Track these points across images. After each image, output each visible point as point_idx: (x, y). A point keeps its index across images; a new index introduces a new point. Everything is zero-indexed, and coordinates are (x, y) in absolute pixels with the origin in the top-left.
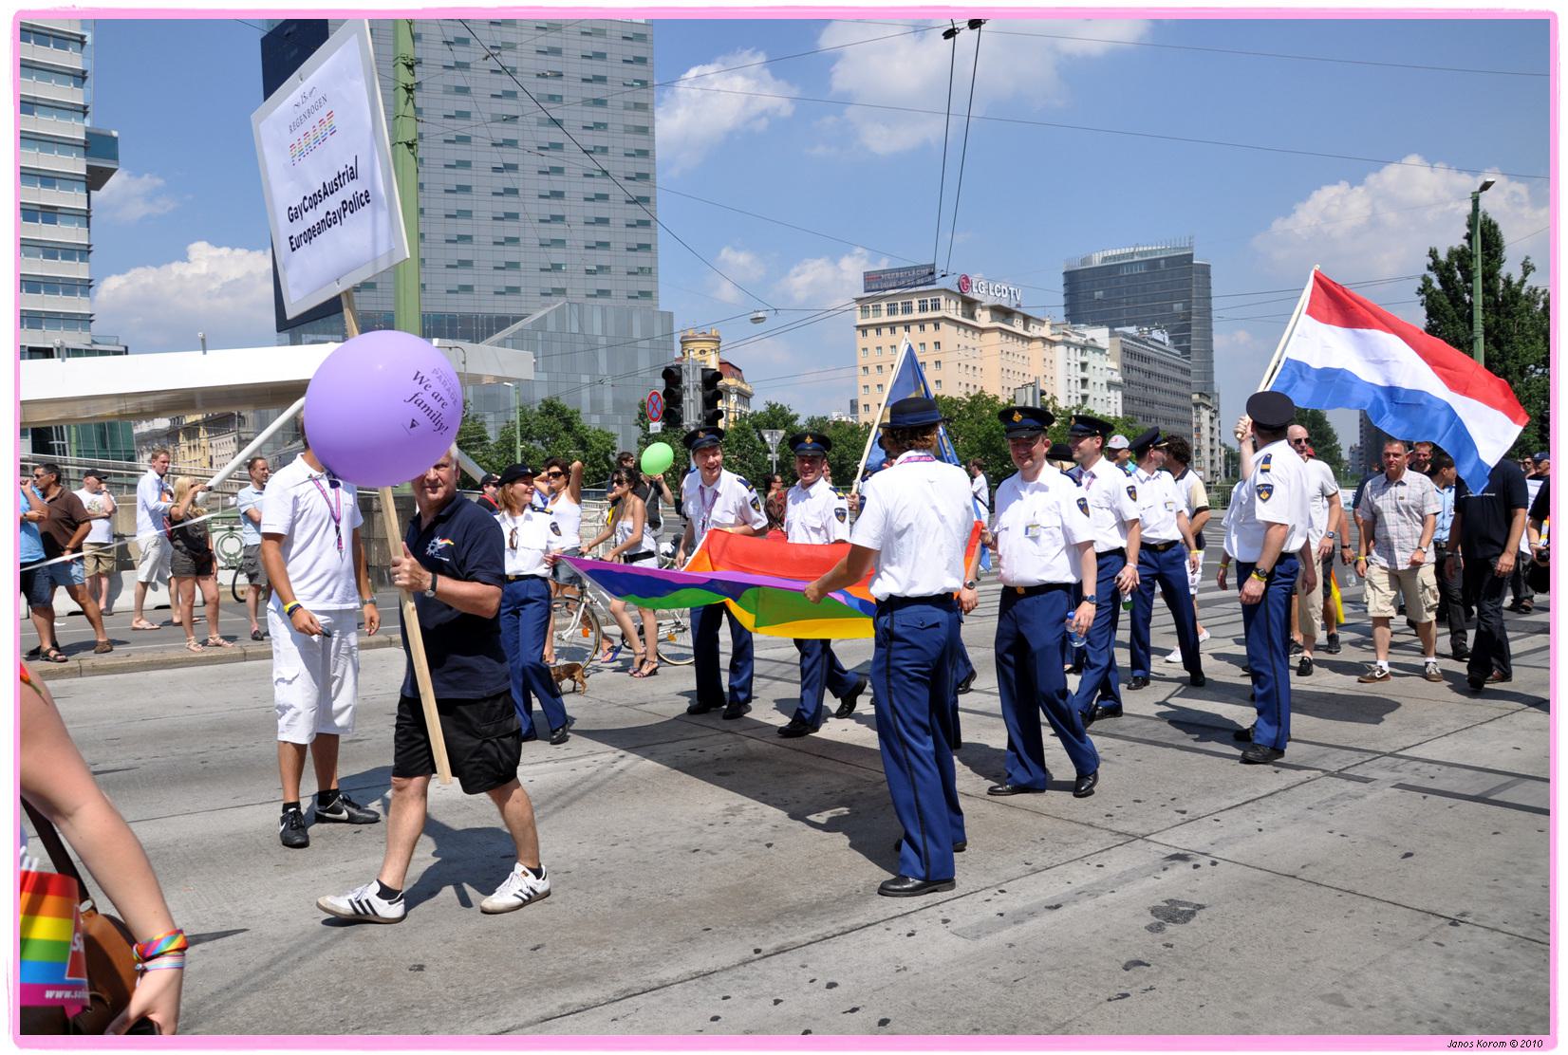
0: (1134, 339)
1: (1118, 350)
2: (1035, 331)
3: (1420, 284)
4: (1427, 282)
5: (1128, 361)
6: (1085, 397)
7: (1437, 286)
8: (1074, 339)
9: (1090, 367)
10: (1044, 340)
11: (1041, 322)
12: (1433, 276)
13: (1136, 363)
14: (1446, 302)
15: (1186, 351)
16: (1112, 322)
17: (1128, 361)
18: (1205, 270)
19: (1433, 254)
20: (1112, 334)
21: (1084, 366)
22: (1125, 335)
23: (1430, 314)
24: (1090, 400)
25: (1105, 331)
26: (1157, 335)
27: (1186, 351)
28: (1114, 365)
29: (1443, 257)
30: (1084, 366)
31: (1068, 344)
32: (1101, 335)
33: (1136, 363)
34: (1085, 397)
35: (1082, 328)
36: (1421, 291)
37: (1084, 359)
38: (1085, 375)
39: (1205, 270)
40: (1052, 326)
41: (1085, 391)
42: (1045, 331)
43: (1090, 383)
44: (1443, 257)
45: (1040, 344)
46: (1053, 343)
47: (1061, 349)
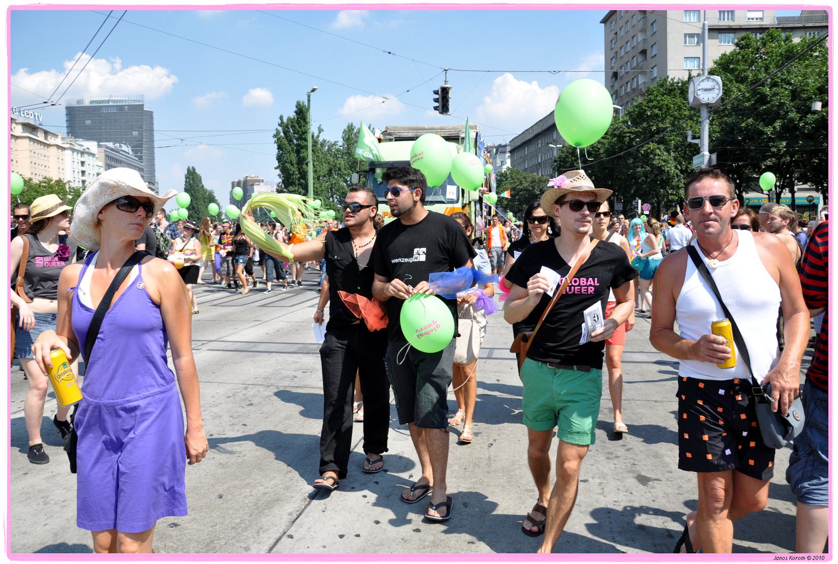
0: (112, 149)
1: (103, 155)
2: (51, 140)
3: (275, 132)
4: (278, 132)
5: (109, 162)
6: (84, 182)
7: (282, 134)
8: (77, 147)
9: (86, 164)
10: (58, 147)
11: (56, 136)
12: (280, 129)
13: (113, 163)
14: (286, 143)
15: (140, 158)
16: (99, 141)
17: (109, 162)
18: (150, 114)
19: (281, 118)
20: (99, 146)
21: (83, 163)
22: (107, 147)
23: (280, 148)
24: (87, 183)
25: (95, 143)
26: (124, 148)
27: (140, 158)
28: (101, 164)
29: (285, 120)
30: (83, 163)
31: (73, 150)
32: (92, 146)
33: (113, 163)
34: (84, 182)
35: (81, 141)
36: (275, 136)
37: (83, 159)
38: (83, 169)
39: (150, 114)
40: (63, 139)
41: (83, 178)
42: (59, 141)
43: (87, 174)
44: (285, 120)
45: (54, 149)
46: (63, 149)
47: (68, 152)
